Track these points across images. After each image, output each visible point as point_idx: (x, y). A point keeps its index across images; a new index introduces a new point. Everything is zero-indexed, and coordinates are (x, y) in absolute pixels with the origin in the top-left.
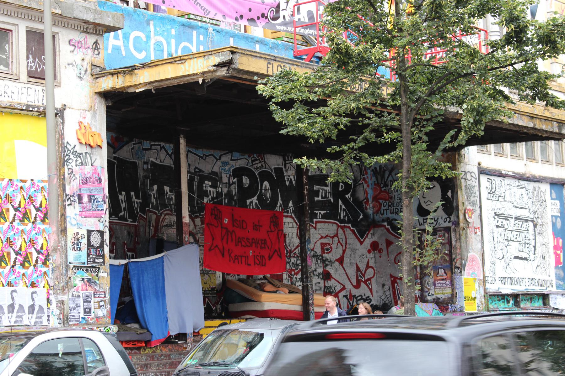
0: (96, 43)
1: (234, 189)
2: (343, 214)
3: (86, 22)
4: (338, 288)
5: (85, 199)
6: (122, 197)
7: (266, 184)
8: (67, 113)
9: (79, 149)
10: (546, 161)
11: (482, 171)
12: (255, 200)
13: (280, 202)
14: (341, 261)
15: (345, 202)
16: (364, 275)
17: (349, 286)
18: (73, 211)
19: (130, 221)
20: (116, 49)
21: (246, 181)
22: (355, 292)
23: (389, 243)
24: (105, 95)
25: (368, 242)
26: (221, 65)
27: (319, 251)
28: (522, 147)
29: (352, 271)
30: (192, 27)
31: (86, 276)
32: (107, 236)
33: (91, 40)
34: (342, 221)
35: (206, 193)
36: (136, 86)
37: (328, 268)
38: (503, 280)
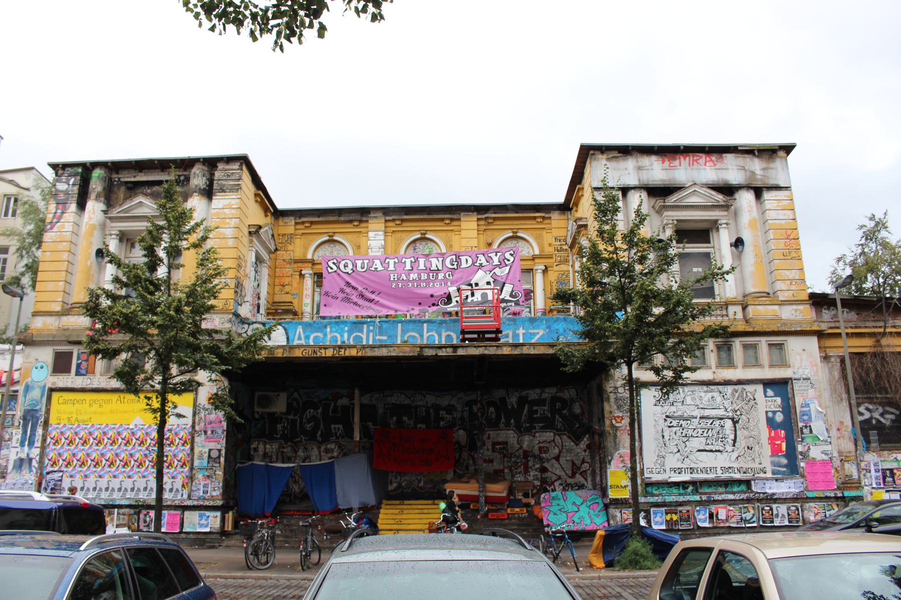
1: (466, 415)
2: (559, 425)
4: (554, 478)
5: (209, 432)
7: (492, 409)
13: (503, 420)
14: (557, 458)
15: (562, 416)
16: (579, 469)
17: (565, 477)
18: (198, 439)
22: (569, 481)
27: (537, 452)
30: (363, 323)
31: (206, 473)
32: (223, 452)
34: (557, 430)
35: (443, 419)
37: (546, 465)
38: (674, 470)
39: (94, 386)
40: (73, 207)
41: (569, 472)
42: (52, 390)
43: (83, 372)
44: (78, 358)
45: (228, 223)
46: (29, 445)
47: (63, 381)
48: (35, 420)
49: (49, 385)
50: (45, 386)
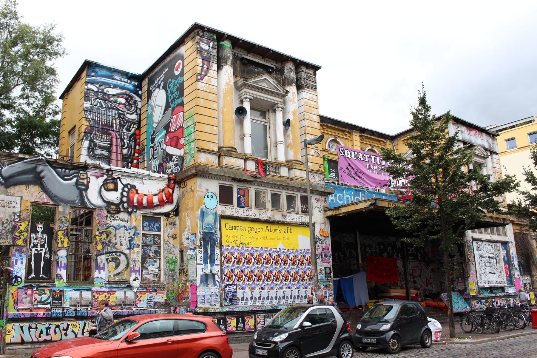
0: (325, 199)
2: (420, 258)
3: (321, 191)
4: (419, 287)
5: (323, 256)
6: (336, 254)
7: (390, 248)
8: (316, 225)
9: (320, 238)
10: (499, 234)
11: (474, 239)
12: (386, 254)
13: (395, 254)
14: (420, 276)
15: (421, 253)
17: (424, 286)
18: (319, 261)
19: (339, 264)
20: (332, 200)
21: (382, 247)
22: (426, 288)
23: (438, 269)
24: (329, 218)
25: (430, 268)
26: (371, 205)
27: (411, 272)
28: (489, 230)
29: (424, 280)
30: (359, 191)
31: (325, 284)
32: (332, 270)
33: (323, 198)
34: (419, 261)
35: (367, 252)
36: (340, 214)
37: (415, 279)
38: (485, 282)
39: (252, 217)
40: (215, 67)
41: (426, 284)
42: (223, 217)
43: (242, 204)
44: (238, 194)
45: (313, 111)
46: (210, 263)
47: (229, 210)
48: (212, 241)
49: (219, 213)
50: (216, 213)
